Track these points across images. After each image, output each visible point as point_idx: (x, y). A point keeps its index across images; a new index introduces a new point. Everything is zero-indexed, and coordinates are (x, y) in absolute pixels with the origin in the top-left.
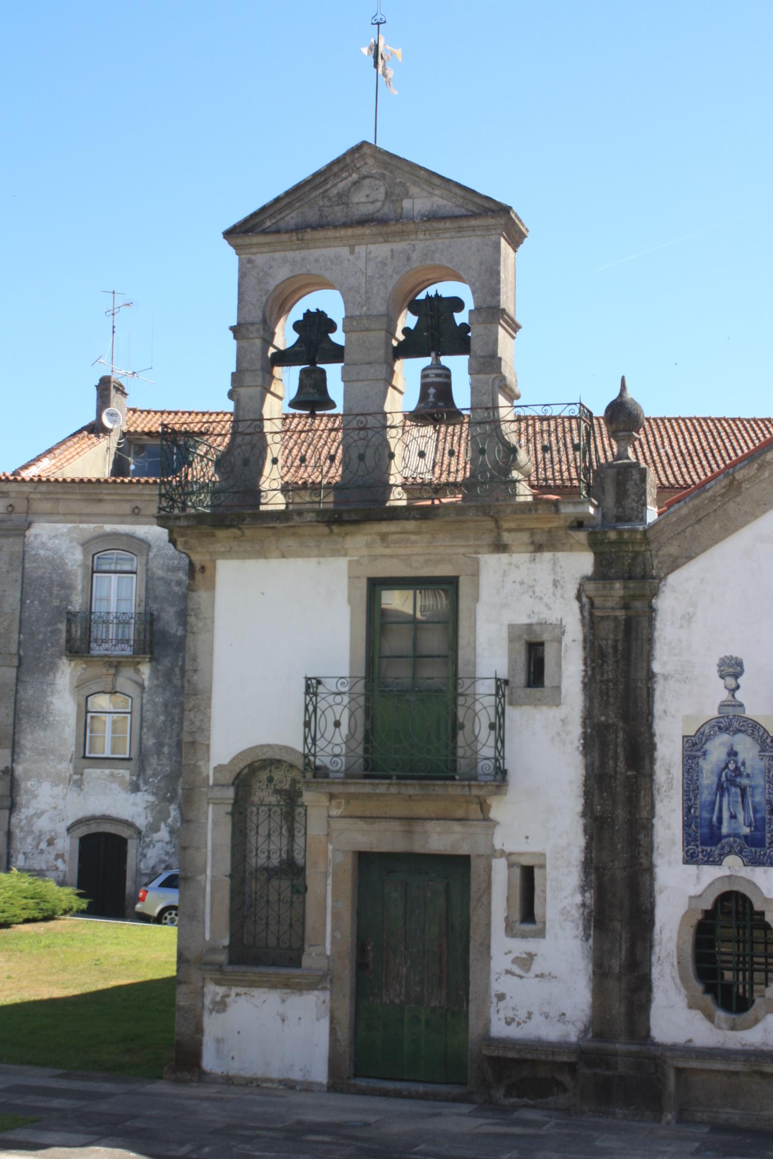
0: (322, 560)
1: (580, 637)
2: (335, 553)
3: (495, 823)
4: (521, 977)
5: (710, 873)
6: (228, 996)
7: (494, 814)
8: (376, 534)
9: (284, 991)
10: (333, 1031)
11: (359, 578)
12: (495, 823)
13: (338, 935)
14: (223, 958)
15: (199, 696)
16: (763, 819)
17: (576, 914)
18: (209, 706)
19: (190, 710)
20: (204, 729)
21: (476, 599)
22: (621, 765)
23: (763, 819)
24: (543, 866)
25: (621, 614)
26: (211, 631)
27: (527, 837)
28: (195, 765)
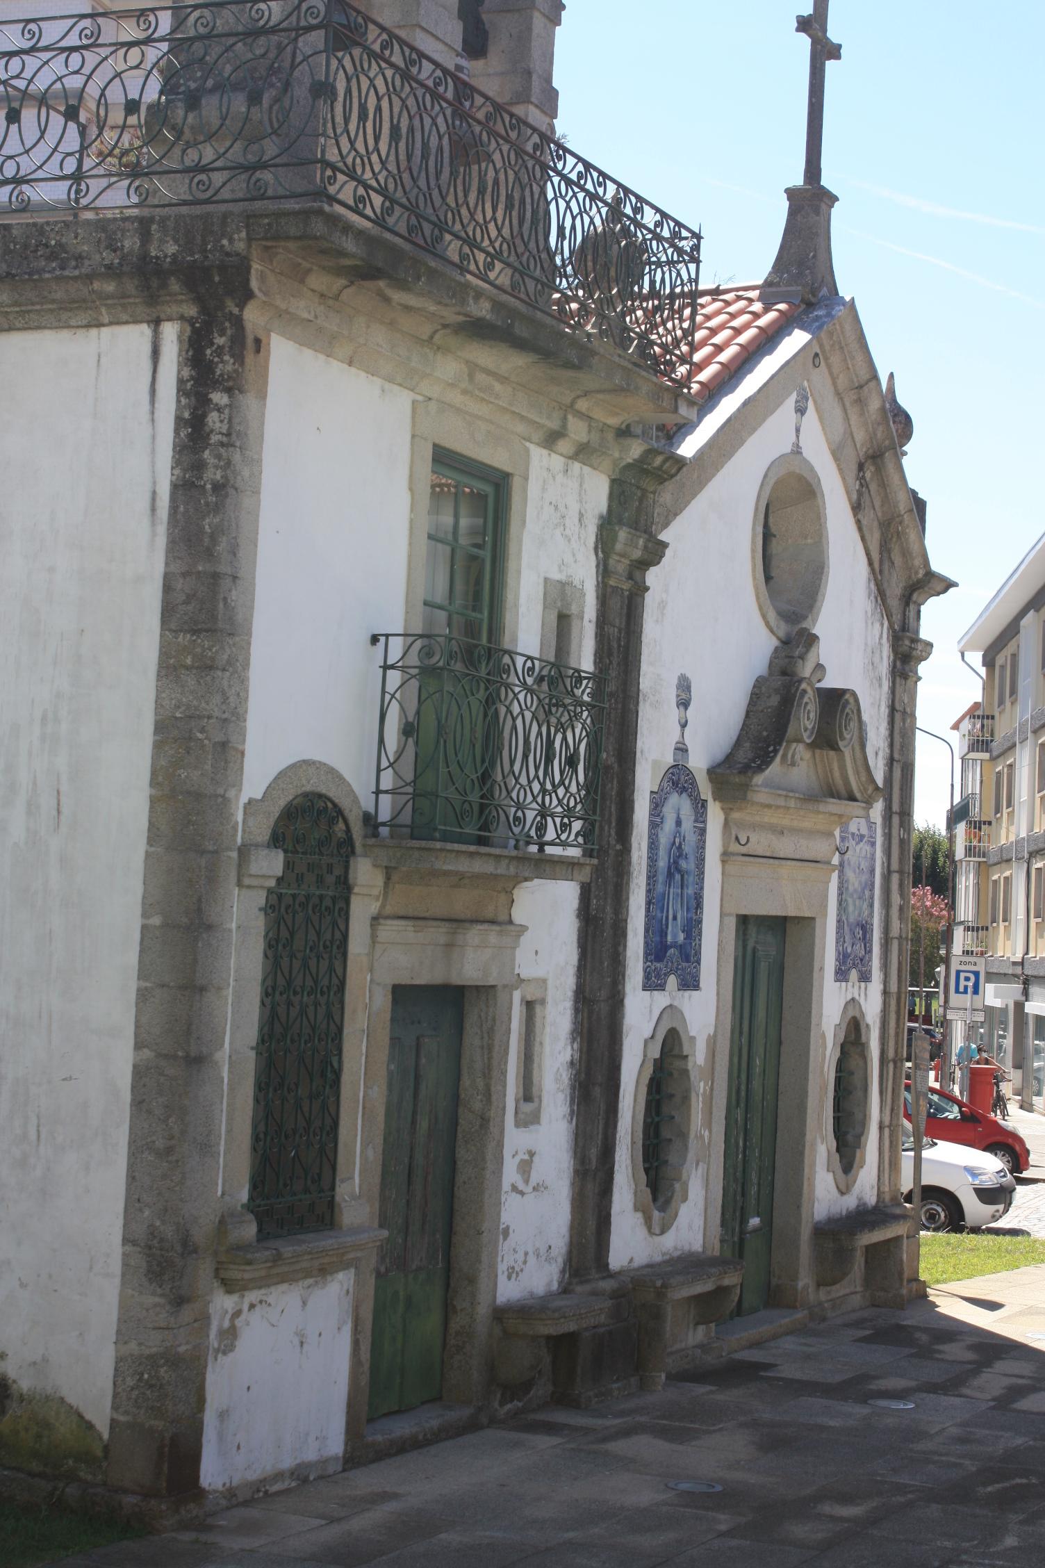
0: (387, 385)
1: (594, 619)
2: (407, 378)
3: (523, 929)
4: (522, 1193)
5: (661, 1000)
6: (238, 1314)
7: (518, 915)
8: (467, 362)
9: (311, 1281)
10: (356, 1344)
11: (426, 439)
12: (523, 929)
13: (370, 1153)
14: (250, 1230)
15: (237, 639)
16: (691, 918)
17: (566, 1077)
18: (246, 665)
19: (224, 670)
20: (234, 717)
21: (523, 523)
22: (613, 832)
23: (691, 918)
24: (543, 1002)
25: (626, 586)
26: (257, 492)
27: (537, 952)
28: (223, 796)
